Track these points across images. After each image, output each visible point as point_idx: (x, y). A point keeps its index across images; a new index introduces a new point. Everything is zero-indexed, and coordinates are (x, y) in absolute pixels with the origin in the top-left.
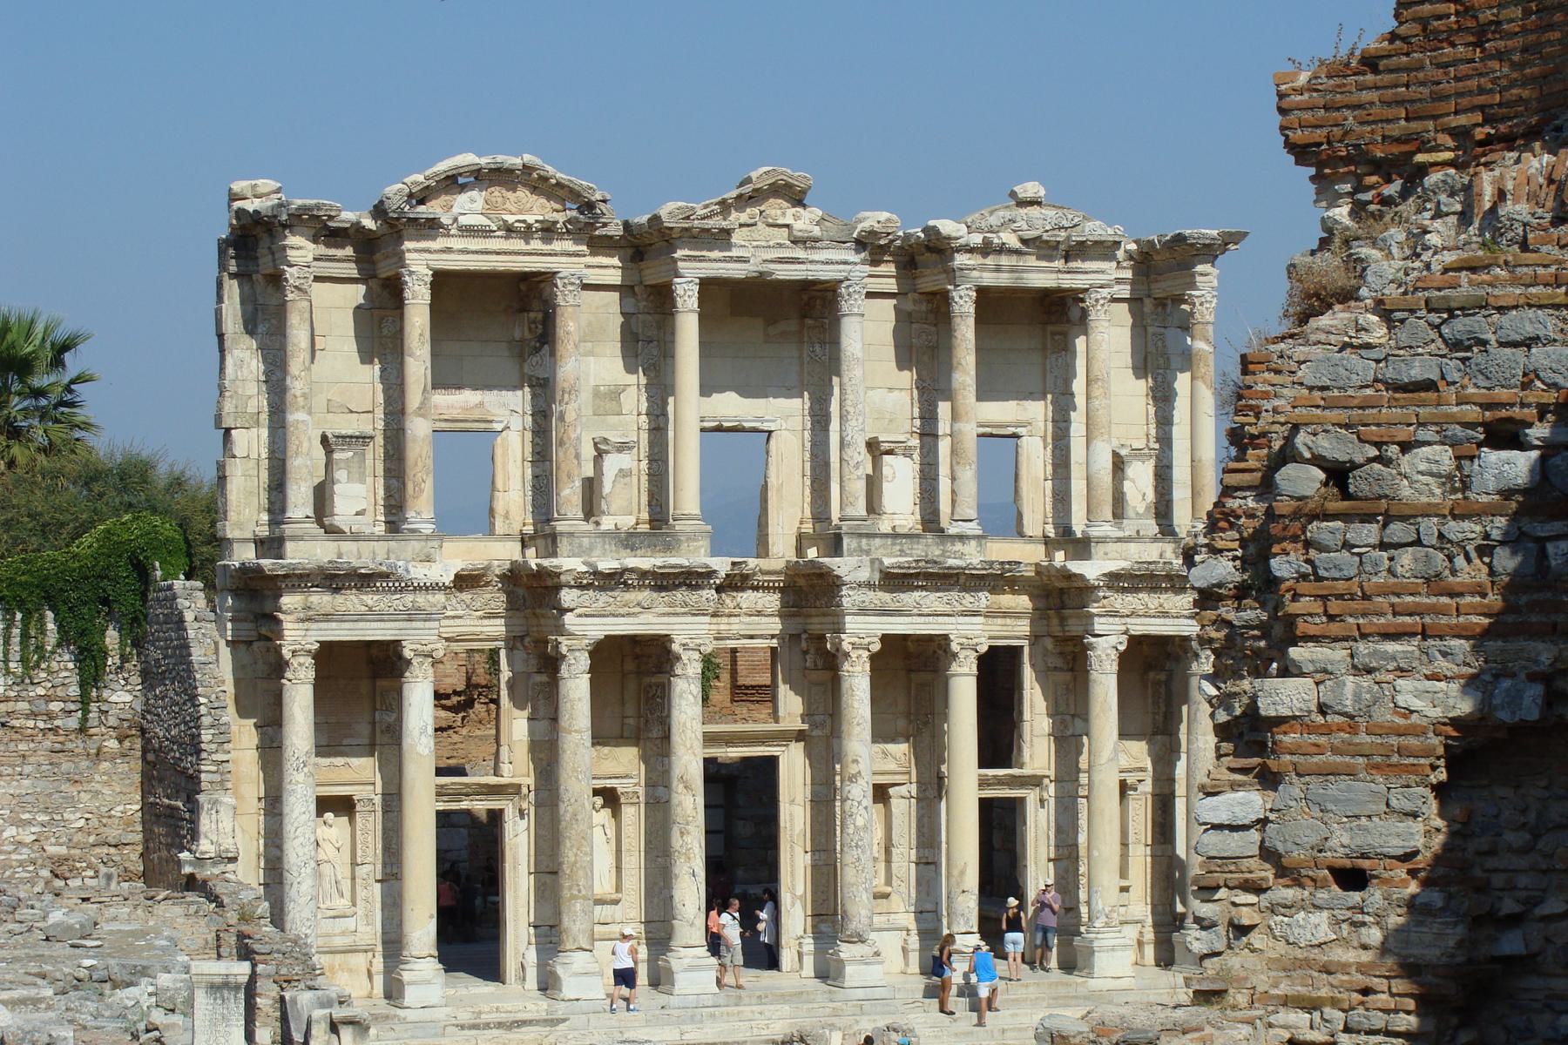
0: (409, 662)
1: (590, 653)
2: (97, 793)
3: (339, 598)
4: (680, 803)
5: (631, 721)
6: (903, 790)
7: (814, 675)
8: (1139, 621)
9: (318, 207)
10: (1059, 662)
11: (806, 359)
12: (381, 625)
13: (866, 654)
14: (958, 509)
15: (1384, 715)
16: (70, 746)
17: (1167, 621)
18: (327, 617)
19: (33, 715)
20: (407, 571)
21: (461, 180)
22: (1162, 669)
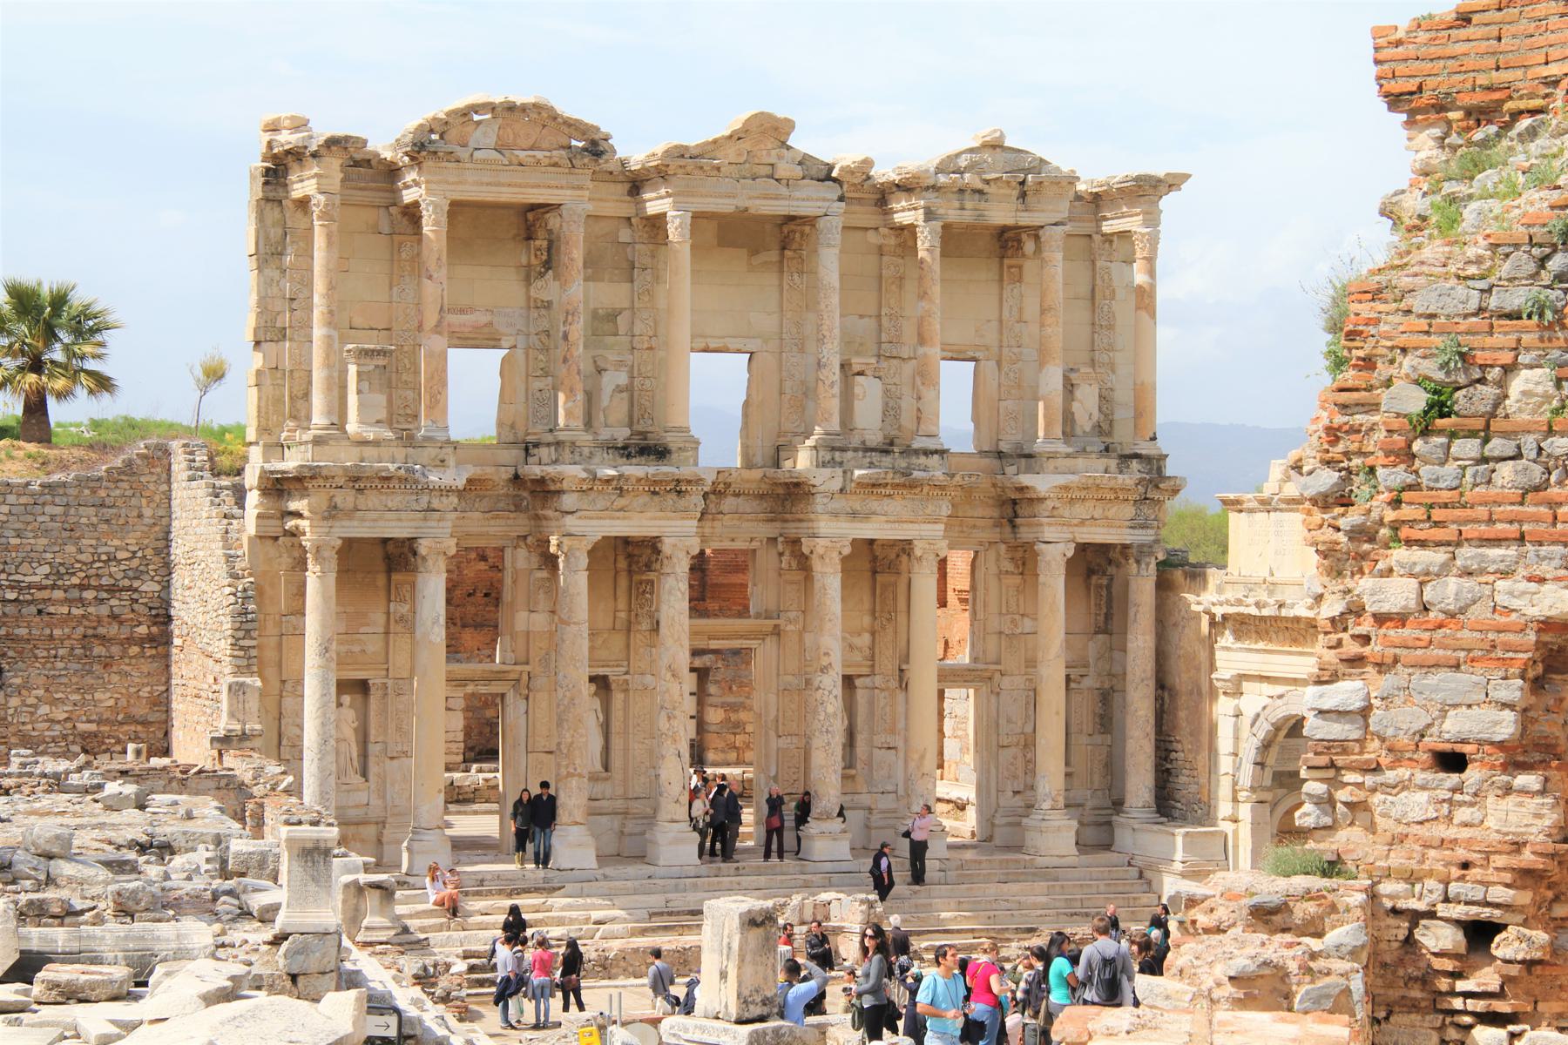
0: (424, 558)
1: (590, 553)
2: (127, 674)
5: (623, 615)
7: (788, 577)
8: (1085, 530)
9: (347, 138)
10: (1009, 566)
11: (786, 287)
13: (836, 559)
14: (922, 426)
15: (1479, 612)
16: (101, 631)
17: (1112, 531)
19: (68, 601)
21: (476, 118)
22: (1104, 574)
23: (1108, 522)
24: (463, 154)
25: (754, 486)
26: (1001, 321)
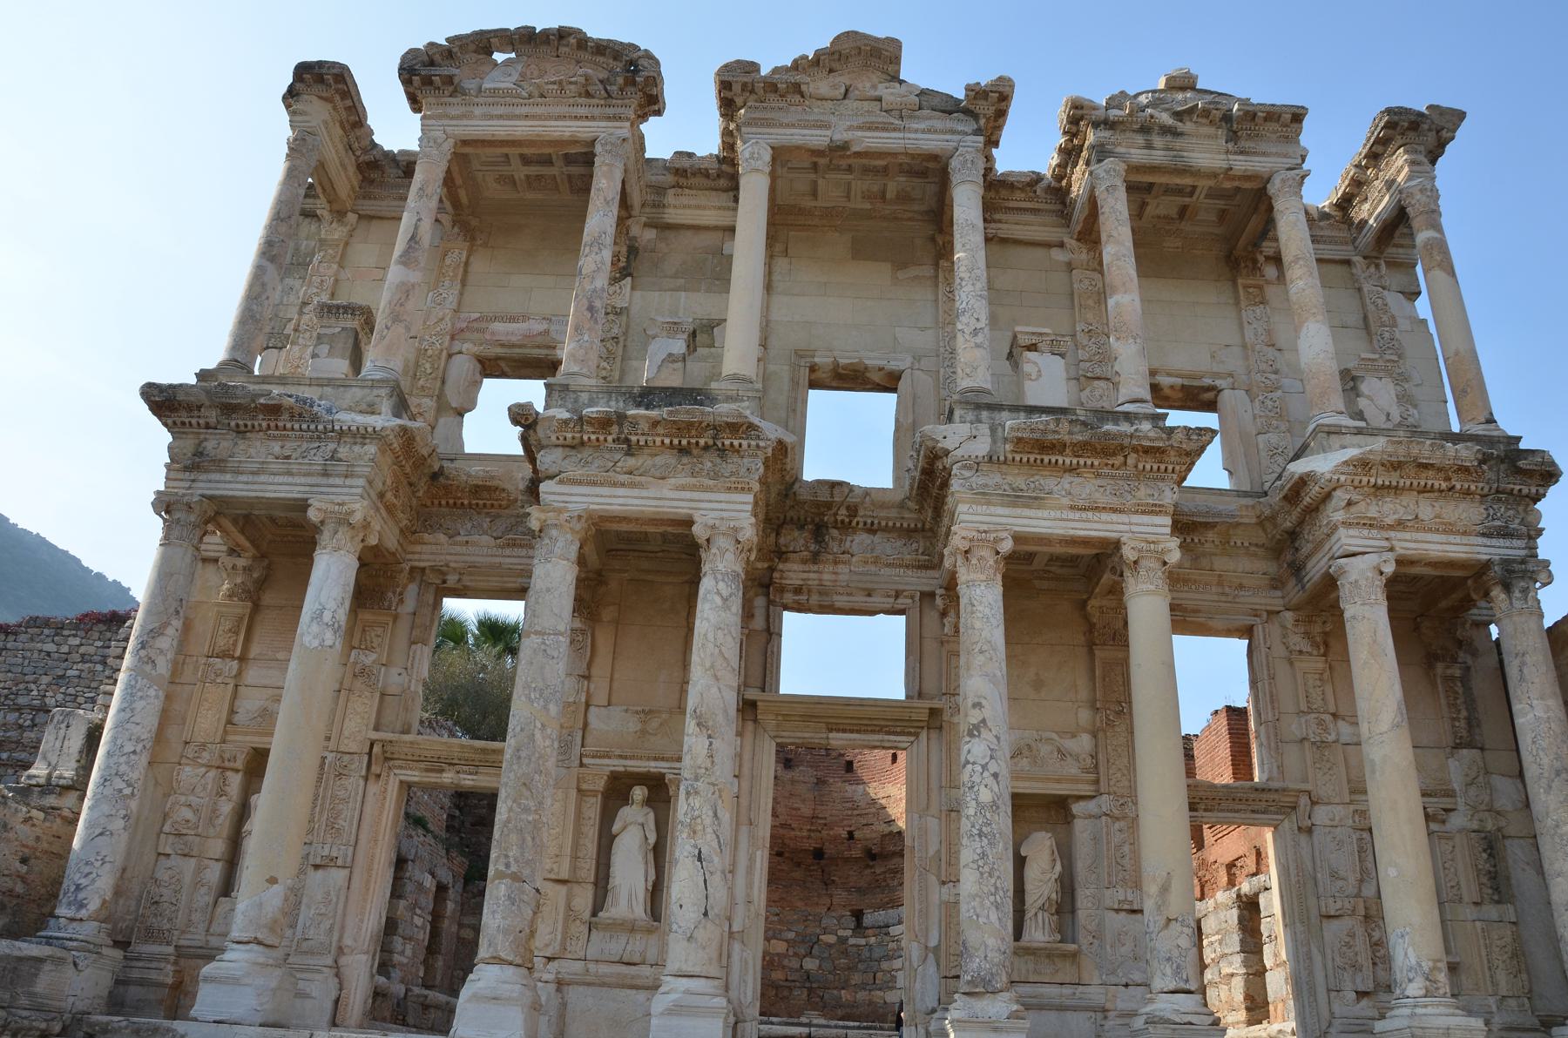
3: (242, 445)
4: (690, 750)
6: (1091, 806)
8: (1408, 536)
9: (320, 64)
10: (1298, 642)
12: (290, 479)
17: (1452, 538)
18: (220, 465)
20: (329, 411)
22: (1454, 660)
23: (1449, 529)
24: (470, 85)
25: (893, 513)
26: (1244, 346)
